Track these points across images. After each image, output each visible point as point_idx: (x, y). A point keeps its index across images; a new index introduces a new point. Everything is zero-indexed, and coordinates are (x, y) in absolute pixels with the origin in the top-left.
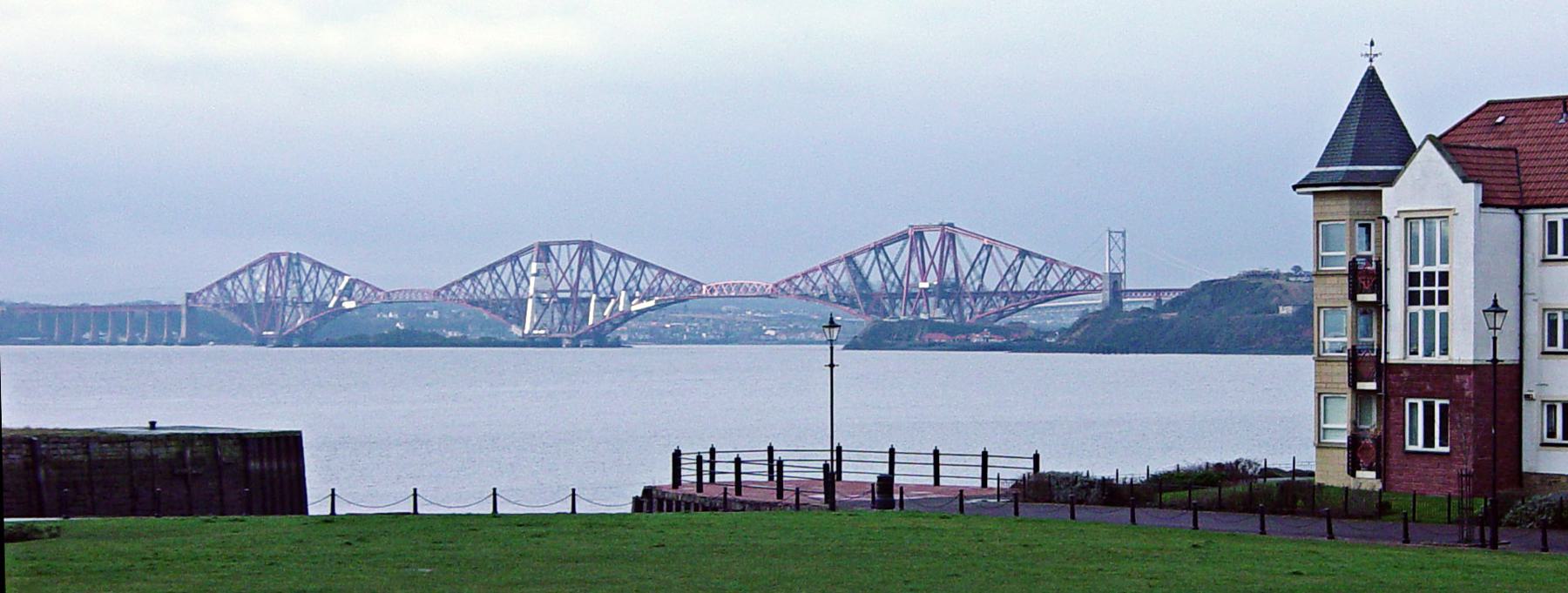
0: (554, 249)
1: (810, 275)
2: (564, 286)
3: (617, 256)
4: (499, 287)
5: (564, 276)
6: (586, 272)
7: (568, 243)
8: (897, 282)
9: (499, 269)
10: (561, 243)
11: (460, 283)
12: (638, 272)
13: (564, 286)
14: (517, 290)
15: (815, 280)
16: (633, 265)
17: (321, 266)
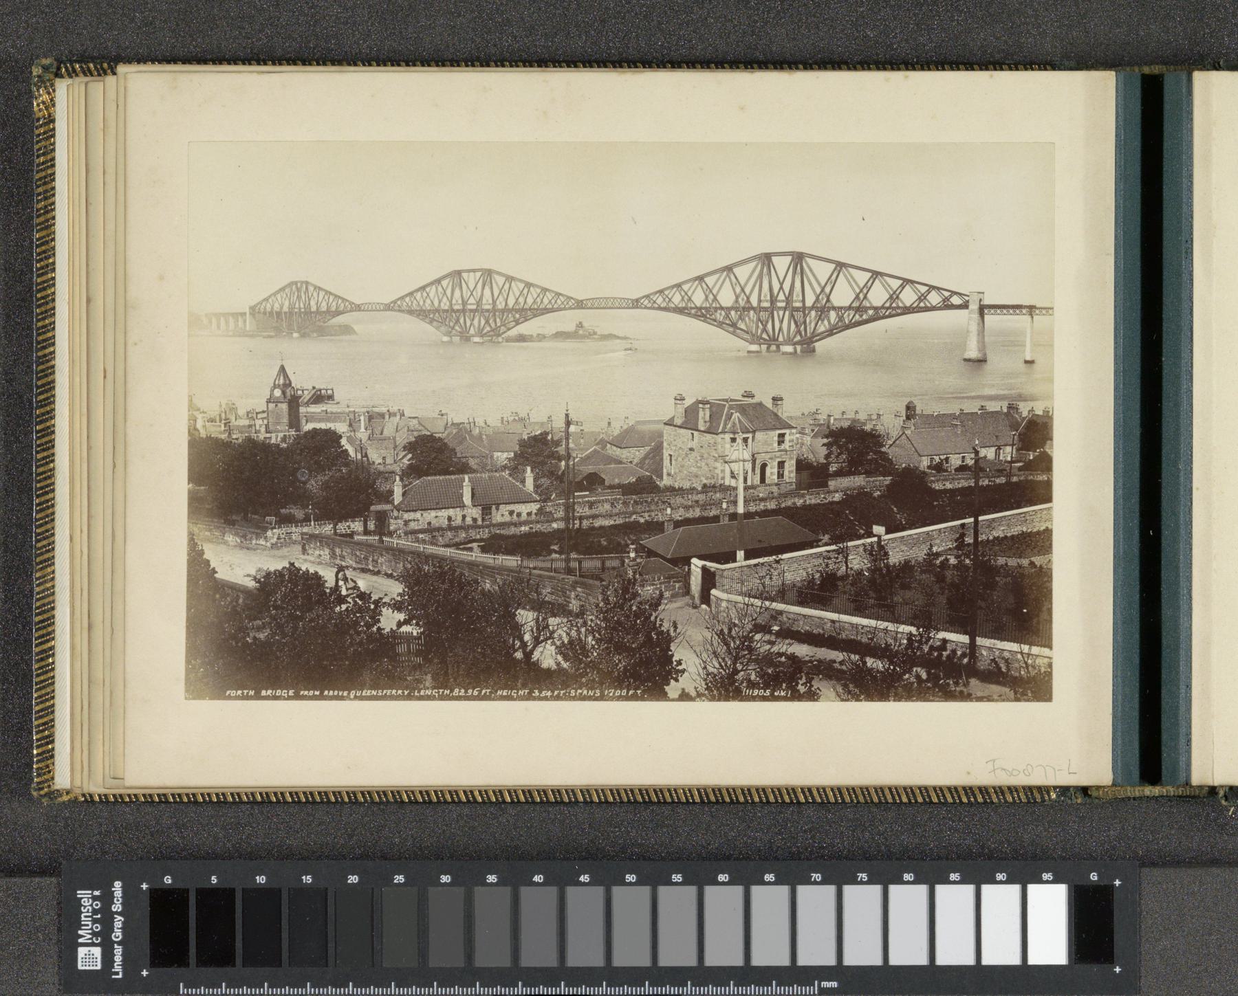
0: (465, 275)
1: (666, 293)
2: (472, 300)
3: (510, 279)
4: (428, 301)
5: (472, 294)
6: (487, 291)
7: (474, 271)
8: (745, 298)
9: (428, 290)
10: (469, 271)
11: (402, 298)
12: (525, 291)
13: (472, 300)
14: (440, 302)
15: (670, 297)
16: (521, 286)
17: (320, 289)
